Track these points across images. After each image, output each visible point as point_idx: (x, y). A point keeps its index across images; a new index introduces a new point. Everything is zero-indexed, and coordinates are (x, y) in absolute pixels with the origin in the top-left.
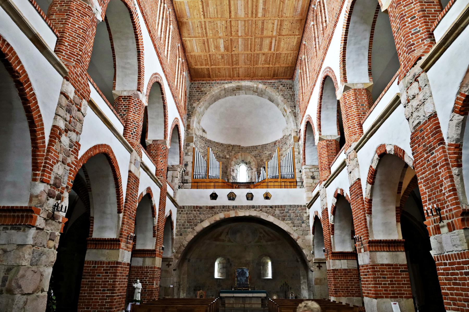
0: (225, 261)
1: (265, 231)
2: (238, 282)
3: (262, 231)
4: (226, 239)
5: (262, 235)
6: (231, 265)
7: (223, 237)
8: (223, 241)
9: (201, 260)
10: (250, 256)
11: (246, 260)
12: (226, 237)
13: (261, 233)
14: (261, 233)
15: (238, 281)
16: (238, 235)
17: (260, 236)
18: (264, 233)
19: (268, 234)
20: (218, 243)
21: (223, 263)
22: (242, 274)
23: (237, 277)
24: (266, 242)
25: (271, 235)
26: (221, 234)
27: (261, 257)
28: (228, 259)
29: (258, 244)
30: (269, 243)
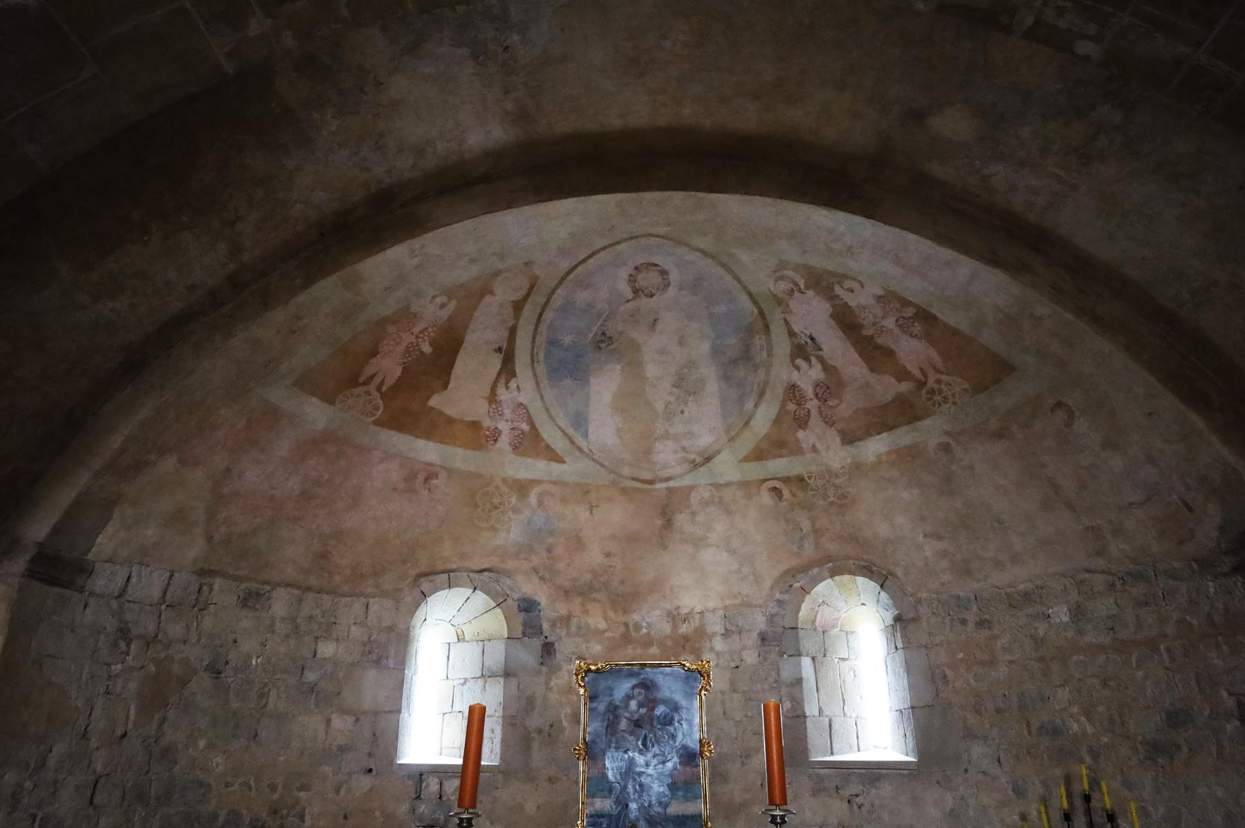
0: (496, 623)
1: (846, 321)
2: (604, 804)
3: (812, 315)
4: (503, 426)
5: (809, 376)
6: (548, 649)
7: (463, 396)
8: (477, 436)
9: (250, 600)
10: (703, 583)
11: (674, 617)
12: (492, 398)
13: (803, 350)
14: (803, 350)
15: (599, 785)
16: (605, 387)
17: (792, 390)
18: (834, 345)
19: (874, 353)
20: (428, 451)
21: (484, 641)
22: (637, 724)
23: (592, 753)
24: (849, 439)
25: (912, 351)
26: (448, 346)
27: (797, 579)
28: (528, 606)
29: (779, 466)
30: (876, 447)
